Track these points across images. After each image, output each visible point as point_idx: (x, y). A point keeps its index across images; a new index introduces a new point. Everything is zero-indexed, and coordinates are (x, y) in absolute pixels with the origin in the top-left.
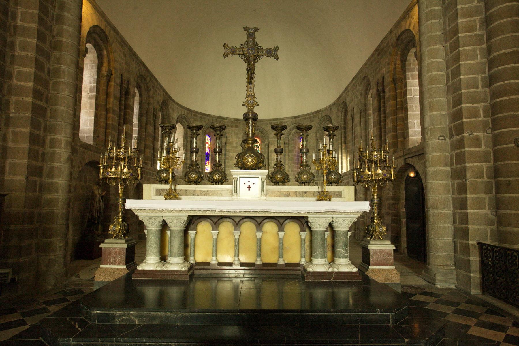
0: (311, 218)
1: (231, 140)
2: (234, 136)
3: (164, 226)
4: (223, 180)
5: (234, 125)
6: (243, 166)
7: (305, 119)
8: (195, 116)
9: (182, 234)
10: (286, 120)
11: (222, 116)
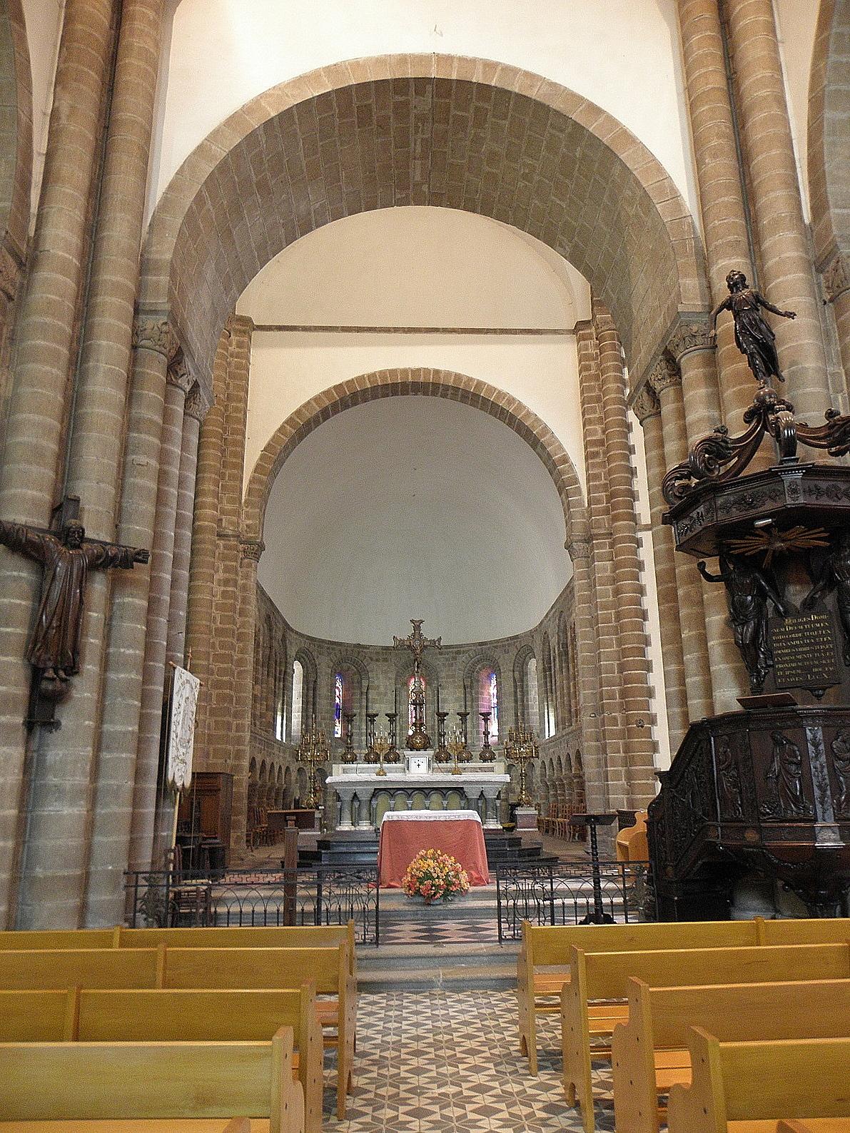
4: (396, 760)
7: (496, 647)
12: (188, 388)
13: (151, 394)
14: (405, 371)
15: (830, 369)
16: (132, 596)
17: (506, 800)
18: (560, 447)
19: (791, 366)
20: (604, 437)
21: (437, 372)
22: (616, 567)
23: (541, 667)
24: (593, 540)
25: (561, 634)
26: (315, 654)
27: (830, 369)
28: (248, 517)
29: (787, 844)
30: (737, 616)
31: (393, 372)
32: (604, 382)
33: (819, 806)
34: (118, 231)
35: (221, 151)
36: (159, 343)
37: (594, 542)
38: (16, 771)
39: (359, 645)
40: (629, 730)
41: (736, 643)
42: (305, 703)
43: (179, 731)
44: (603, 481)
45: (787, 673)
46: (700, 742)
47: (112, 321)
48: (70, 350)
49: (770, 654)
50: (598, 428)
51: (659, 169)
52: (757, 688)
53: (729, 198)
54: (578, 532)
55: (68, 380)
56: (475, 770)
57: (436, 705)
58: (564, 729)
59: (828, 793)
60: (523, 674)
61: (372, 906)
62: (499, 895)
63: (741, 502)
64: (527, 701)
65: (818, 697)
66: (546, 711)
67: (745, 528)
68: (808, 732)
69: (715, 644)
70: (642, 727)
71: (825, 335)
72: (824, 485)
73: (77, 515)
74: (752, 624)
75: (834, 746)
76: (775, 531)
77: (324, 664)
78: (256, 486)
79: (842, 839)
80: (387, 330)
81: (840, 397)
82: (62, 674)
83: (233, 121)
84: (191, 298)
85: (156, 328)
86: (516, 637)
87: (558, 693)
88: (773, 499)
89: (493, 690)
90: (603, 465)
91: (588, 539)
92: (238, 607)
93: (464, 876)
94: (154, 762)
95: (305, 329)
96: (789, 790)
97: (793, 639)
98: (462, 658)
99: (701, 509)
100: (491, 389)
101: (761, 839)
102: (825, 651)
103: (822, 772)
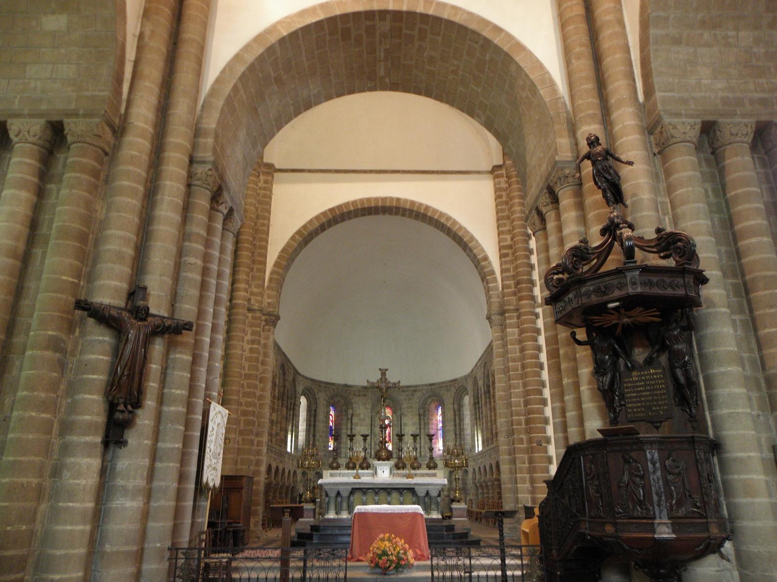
0: (416, 488)
1: (358, 411)
2: (361, 407)
3: (338, 494)
5: (362, 393)
6: (379, 459)
7: (441, 387)
8: (319, 386)
9: (347, 499)
10: (420, 388)
11: (349, 383)
12: (225, 212)
13: (199, 217)
14: (376, 199)
15: (659, 199)
16: (181, 353)
17: (448, 496)
18: (483, 250)
19: (632, 197)
20: (512, 243)
21: (398, 200)
22: (522, 332)
23: (472, 402)
24: (505, 313)
25: (485, 379)
26: (316, 391)
27: (659, 199)
28: (269, 297)
29: (635, 535)
30: (599, 370)
31: (369, 200)
32: (512, 206)
33: (656, 508)
34: (180, 110)
35: (250, 58)
36: (206, 182)
37: (506, 315)
38: (95, 475)
39: (346, 385)
40: (532, 447)
41: (599, 389)
42: (309, 425)
43: (212, 447)
44: (512, 273)
45: (635, 410)
46: (574, 459)
47: (174, 168)
48: (145, 187)
49: (622, 397)
50: (508, 237)
51: (541, 67)
52: (614, 421)
53: (588, 86)
54: (495, 308)
55: (143, 207)
56: (423, 475)
57: (400, 427)
58: (488, 445)
59: (663, 498)
60: (460, 406)
61: (342, 575)
62: (432, 568)
63: (597, 291)
64: (463, 425)
65: (657, 428)
66: (476, 432)
67: (601, 308)
68: (648, 454)
69: (585, 389)
70: (541, 445)
71: (655, 176)
72: (654, 279)
73: (145, 298)
74: (609, 376)
75: (667, 464)
76: (622, 311)
77: (322, 398)
78: (275, 276)
79: (674, 532)
80: (365, 172)
81: (667, 219)
82: (130, 408)
83: (258, 39)
84: (228, 152)
85: (204, 173)
86: (455, 380)
87: (484, 420)
88: (620, 289)
89: (440, 418)
90: (512, 262)
91: (502, 313)
92: (260, 359)
93: (410, 554)
94: (194, 469)
95: (310, 171)
96: (636, 496)
97: (638, 386)
98: (418, 394)
99: (571, 296)
100: (435, 211)
101: (616, 531)
102: (661, 395)
103: (658, 483)
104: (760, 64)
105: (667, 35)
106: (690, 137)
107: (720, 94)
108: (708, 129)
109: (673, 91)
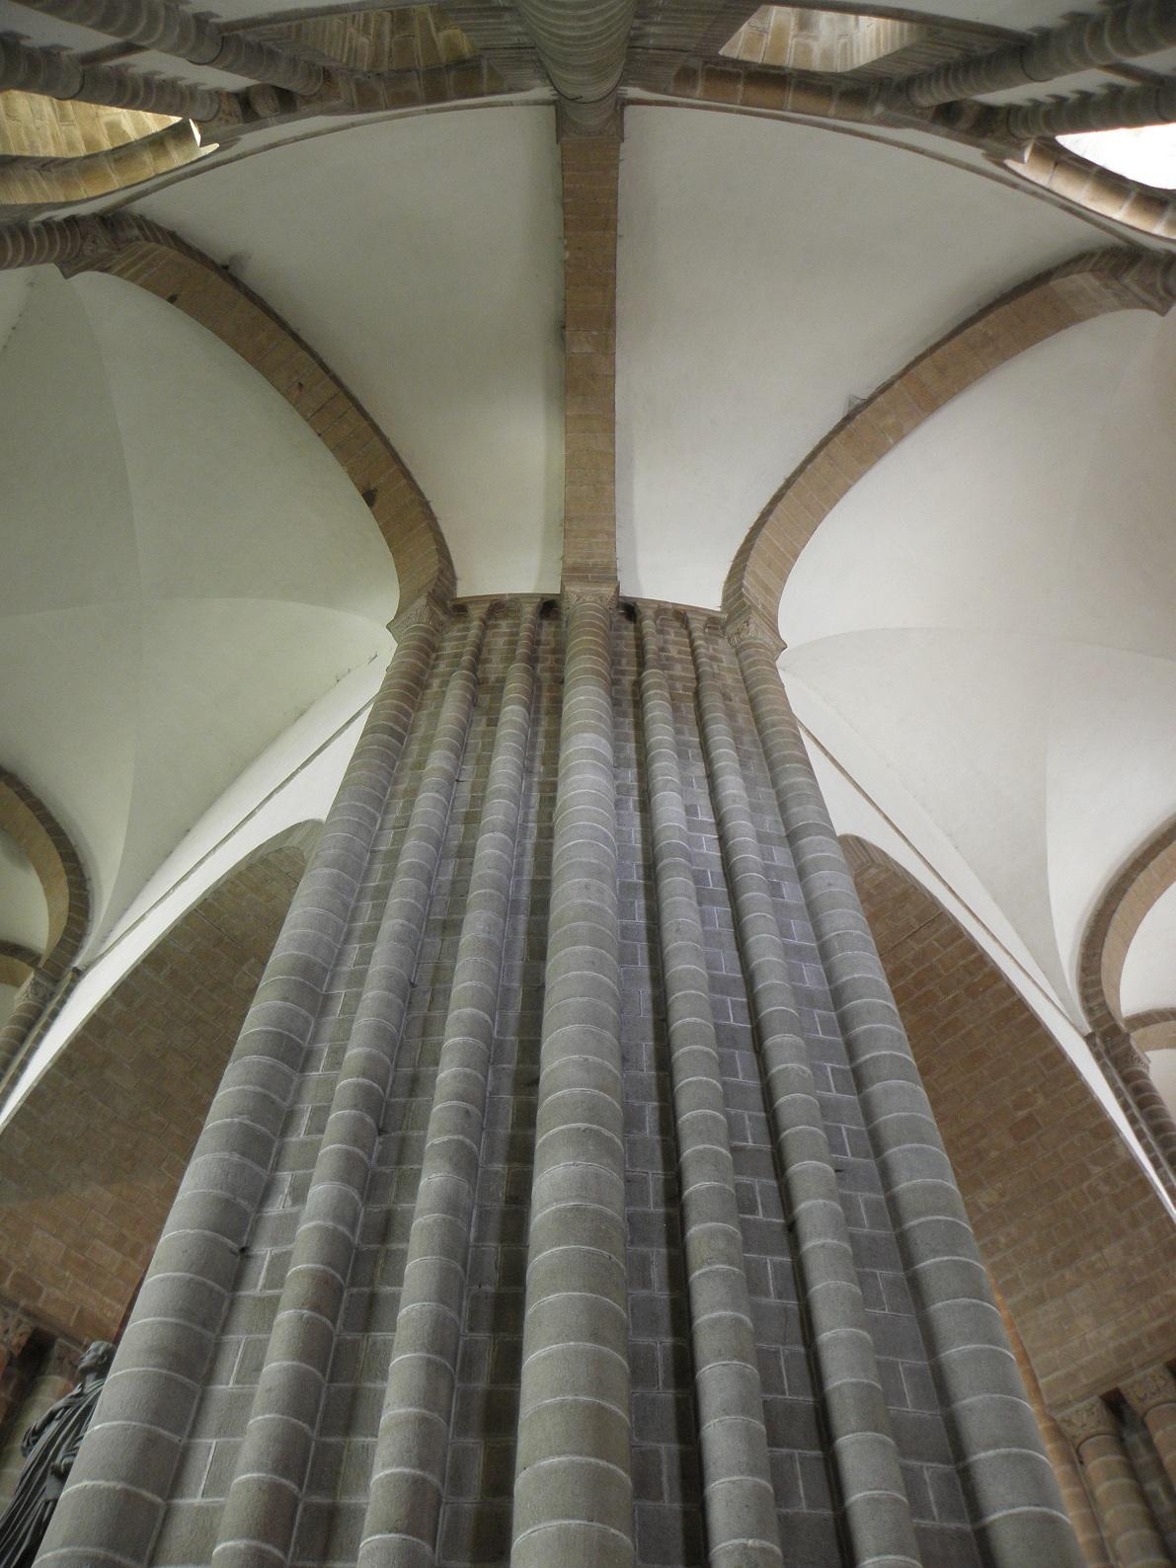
104: (1145, 1277)
105: (1026, 1298)
106: (1093, 1427)
107: (1112, 1345)
108: (1115, 1404)
109: (1056, 1369)
